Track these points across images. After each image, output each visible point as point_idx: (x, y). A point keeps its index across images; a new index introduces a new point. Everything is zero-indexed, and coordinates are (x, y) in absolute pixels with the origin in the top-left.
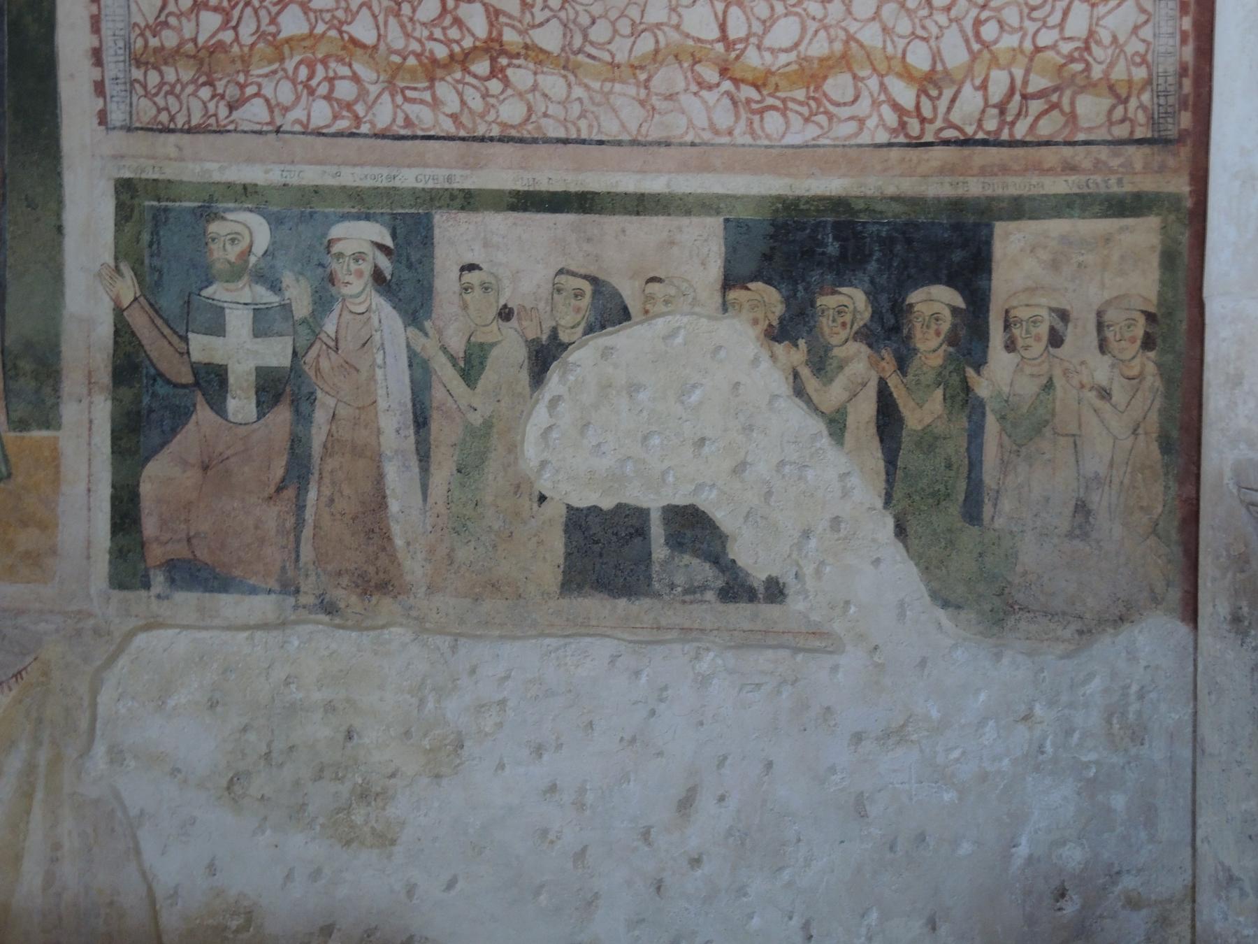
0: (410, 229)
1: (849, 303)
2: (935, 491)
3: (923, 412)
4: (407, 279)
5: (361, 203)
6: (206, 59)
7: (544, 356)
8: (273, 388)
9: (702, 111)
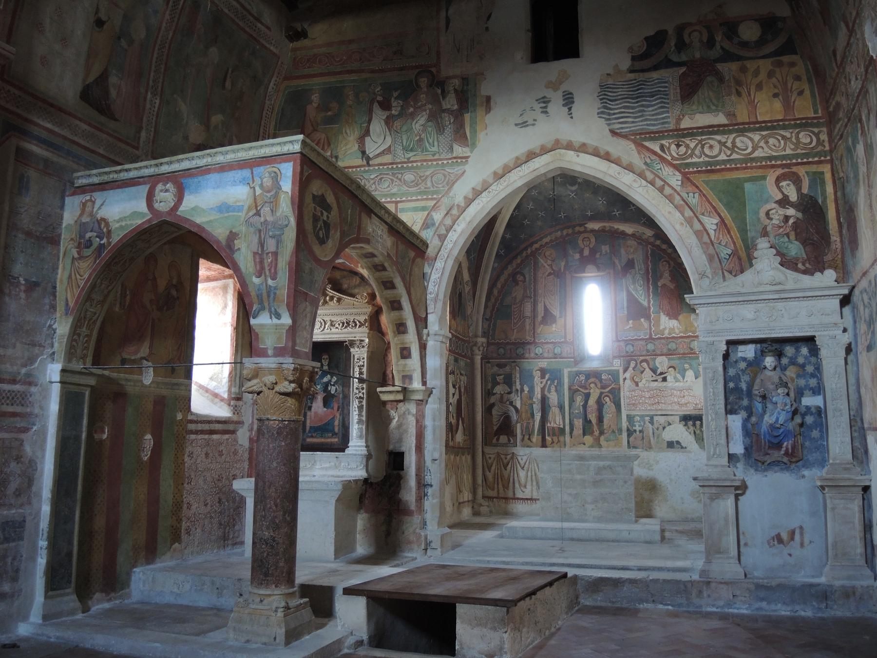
0: (652, 418)
1: (690, 423)
2: (699, 439)
3: (698, 432)
4: (652, 422)
5: (647, 416)
6: (634, 404)
7: (664, 428)
8: (640, 431)
9: (677, 407)
